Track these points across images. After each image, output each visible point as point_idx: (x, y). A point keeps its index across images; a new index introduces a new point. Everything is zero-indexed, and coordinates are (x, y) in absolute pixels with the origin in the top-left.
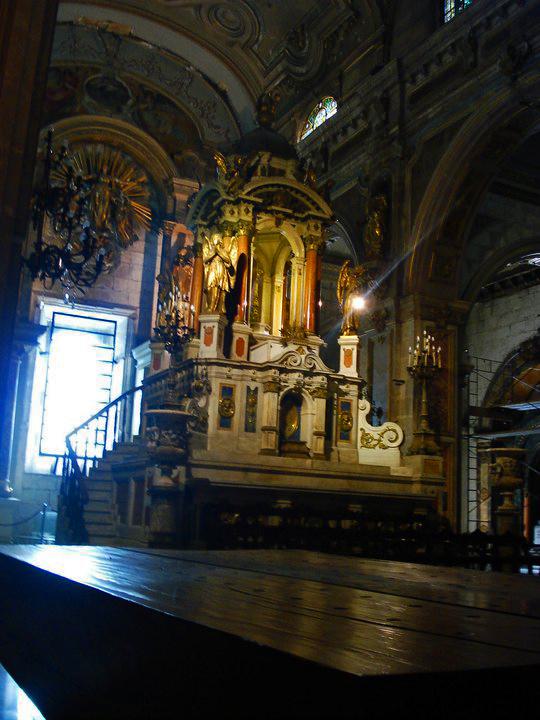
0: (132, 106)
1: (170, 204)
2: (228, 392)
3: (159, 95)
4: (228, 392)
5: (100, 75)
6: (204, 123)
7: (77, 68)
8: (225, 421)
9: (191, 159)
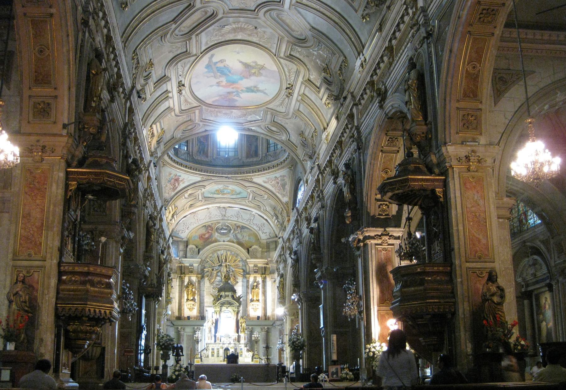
0: (233, 233)
1: (248, 268)
2: (213, 349)
3: (242, 226)
4: (213, 349)
5: (220, 224)
6: (260, 232)
7: (212, 224)
8: (213, 355)
9: (255, 249)
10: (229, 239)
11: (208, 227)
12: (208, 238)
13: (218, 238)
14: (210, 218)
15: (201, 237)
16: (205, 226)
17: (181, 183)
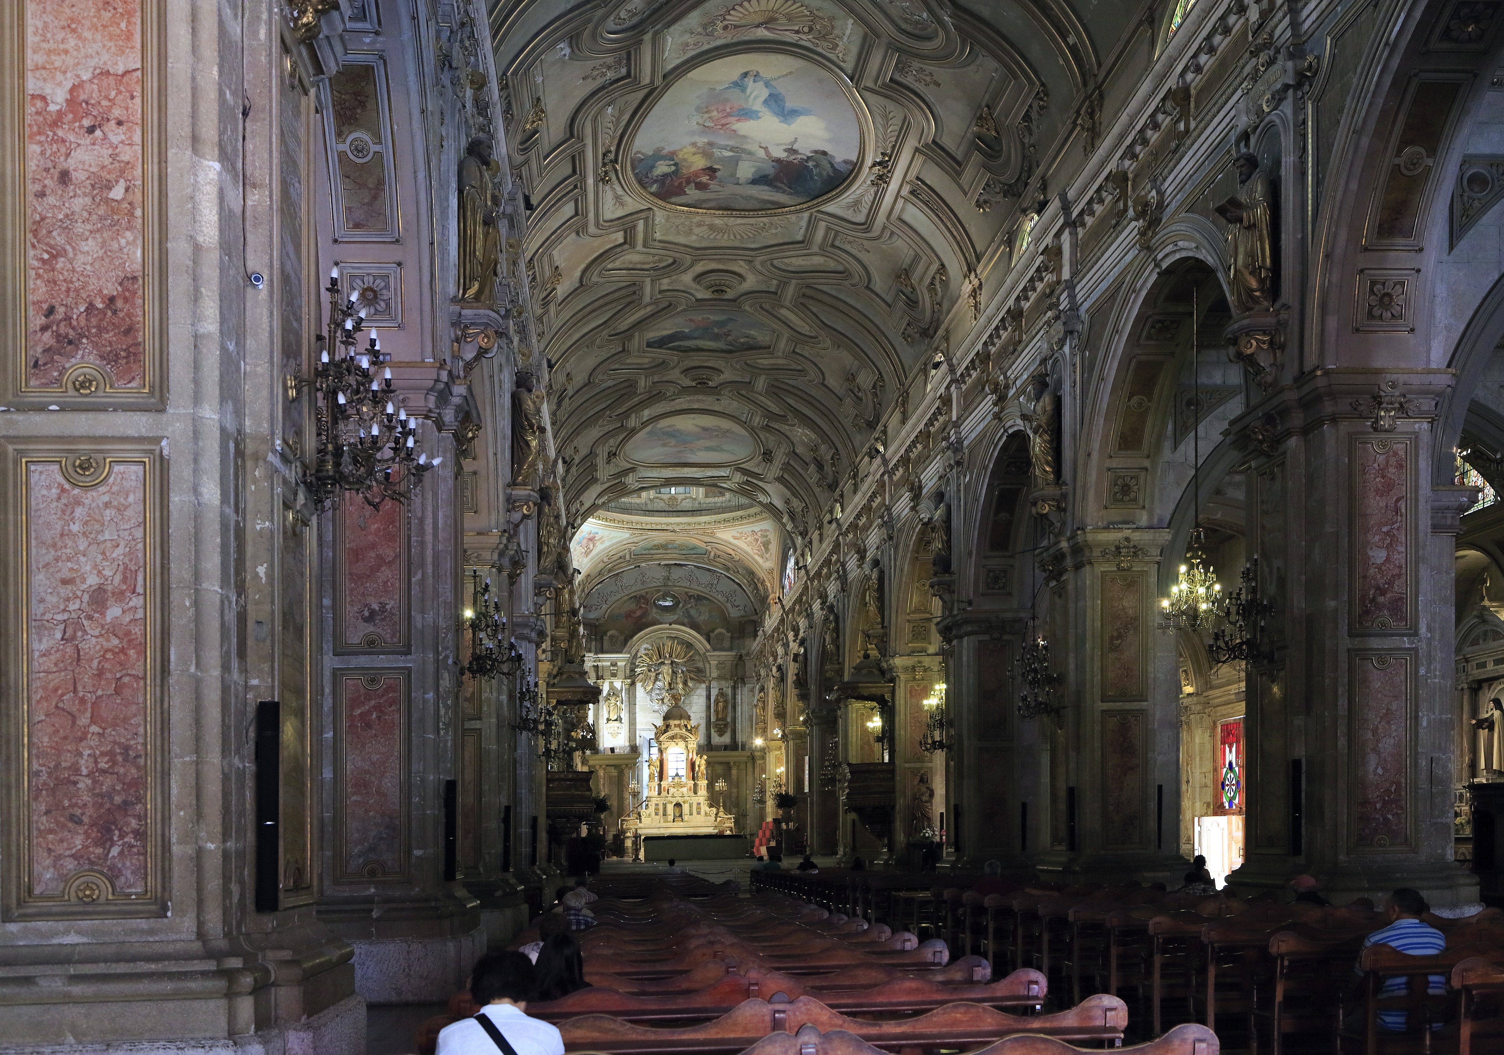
10: (675, 617)
11: (638, 599)
12: (640, 617)
13: (658, 617)
14: (643, 583)
15: (628, 615)
16: (635, 597)
17: (598, 544)
